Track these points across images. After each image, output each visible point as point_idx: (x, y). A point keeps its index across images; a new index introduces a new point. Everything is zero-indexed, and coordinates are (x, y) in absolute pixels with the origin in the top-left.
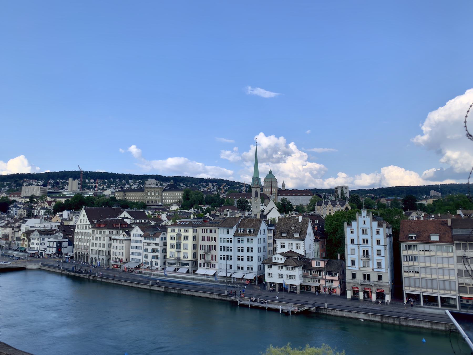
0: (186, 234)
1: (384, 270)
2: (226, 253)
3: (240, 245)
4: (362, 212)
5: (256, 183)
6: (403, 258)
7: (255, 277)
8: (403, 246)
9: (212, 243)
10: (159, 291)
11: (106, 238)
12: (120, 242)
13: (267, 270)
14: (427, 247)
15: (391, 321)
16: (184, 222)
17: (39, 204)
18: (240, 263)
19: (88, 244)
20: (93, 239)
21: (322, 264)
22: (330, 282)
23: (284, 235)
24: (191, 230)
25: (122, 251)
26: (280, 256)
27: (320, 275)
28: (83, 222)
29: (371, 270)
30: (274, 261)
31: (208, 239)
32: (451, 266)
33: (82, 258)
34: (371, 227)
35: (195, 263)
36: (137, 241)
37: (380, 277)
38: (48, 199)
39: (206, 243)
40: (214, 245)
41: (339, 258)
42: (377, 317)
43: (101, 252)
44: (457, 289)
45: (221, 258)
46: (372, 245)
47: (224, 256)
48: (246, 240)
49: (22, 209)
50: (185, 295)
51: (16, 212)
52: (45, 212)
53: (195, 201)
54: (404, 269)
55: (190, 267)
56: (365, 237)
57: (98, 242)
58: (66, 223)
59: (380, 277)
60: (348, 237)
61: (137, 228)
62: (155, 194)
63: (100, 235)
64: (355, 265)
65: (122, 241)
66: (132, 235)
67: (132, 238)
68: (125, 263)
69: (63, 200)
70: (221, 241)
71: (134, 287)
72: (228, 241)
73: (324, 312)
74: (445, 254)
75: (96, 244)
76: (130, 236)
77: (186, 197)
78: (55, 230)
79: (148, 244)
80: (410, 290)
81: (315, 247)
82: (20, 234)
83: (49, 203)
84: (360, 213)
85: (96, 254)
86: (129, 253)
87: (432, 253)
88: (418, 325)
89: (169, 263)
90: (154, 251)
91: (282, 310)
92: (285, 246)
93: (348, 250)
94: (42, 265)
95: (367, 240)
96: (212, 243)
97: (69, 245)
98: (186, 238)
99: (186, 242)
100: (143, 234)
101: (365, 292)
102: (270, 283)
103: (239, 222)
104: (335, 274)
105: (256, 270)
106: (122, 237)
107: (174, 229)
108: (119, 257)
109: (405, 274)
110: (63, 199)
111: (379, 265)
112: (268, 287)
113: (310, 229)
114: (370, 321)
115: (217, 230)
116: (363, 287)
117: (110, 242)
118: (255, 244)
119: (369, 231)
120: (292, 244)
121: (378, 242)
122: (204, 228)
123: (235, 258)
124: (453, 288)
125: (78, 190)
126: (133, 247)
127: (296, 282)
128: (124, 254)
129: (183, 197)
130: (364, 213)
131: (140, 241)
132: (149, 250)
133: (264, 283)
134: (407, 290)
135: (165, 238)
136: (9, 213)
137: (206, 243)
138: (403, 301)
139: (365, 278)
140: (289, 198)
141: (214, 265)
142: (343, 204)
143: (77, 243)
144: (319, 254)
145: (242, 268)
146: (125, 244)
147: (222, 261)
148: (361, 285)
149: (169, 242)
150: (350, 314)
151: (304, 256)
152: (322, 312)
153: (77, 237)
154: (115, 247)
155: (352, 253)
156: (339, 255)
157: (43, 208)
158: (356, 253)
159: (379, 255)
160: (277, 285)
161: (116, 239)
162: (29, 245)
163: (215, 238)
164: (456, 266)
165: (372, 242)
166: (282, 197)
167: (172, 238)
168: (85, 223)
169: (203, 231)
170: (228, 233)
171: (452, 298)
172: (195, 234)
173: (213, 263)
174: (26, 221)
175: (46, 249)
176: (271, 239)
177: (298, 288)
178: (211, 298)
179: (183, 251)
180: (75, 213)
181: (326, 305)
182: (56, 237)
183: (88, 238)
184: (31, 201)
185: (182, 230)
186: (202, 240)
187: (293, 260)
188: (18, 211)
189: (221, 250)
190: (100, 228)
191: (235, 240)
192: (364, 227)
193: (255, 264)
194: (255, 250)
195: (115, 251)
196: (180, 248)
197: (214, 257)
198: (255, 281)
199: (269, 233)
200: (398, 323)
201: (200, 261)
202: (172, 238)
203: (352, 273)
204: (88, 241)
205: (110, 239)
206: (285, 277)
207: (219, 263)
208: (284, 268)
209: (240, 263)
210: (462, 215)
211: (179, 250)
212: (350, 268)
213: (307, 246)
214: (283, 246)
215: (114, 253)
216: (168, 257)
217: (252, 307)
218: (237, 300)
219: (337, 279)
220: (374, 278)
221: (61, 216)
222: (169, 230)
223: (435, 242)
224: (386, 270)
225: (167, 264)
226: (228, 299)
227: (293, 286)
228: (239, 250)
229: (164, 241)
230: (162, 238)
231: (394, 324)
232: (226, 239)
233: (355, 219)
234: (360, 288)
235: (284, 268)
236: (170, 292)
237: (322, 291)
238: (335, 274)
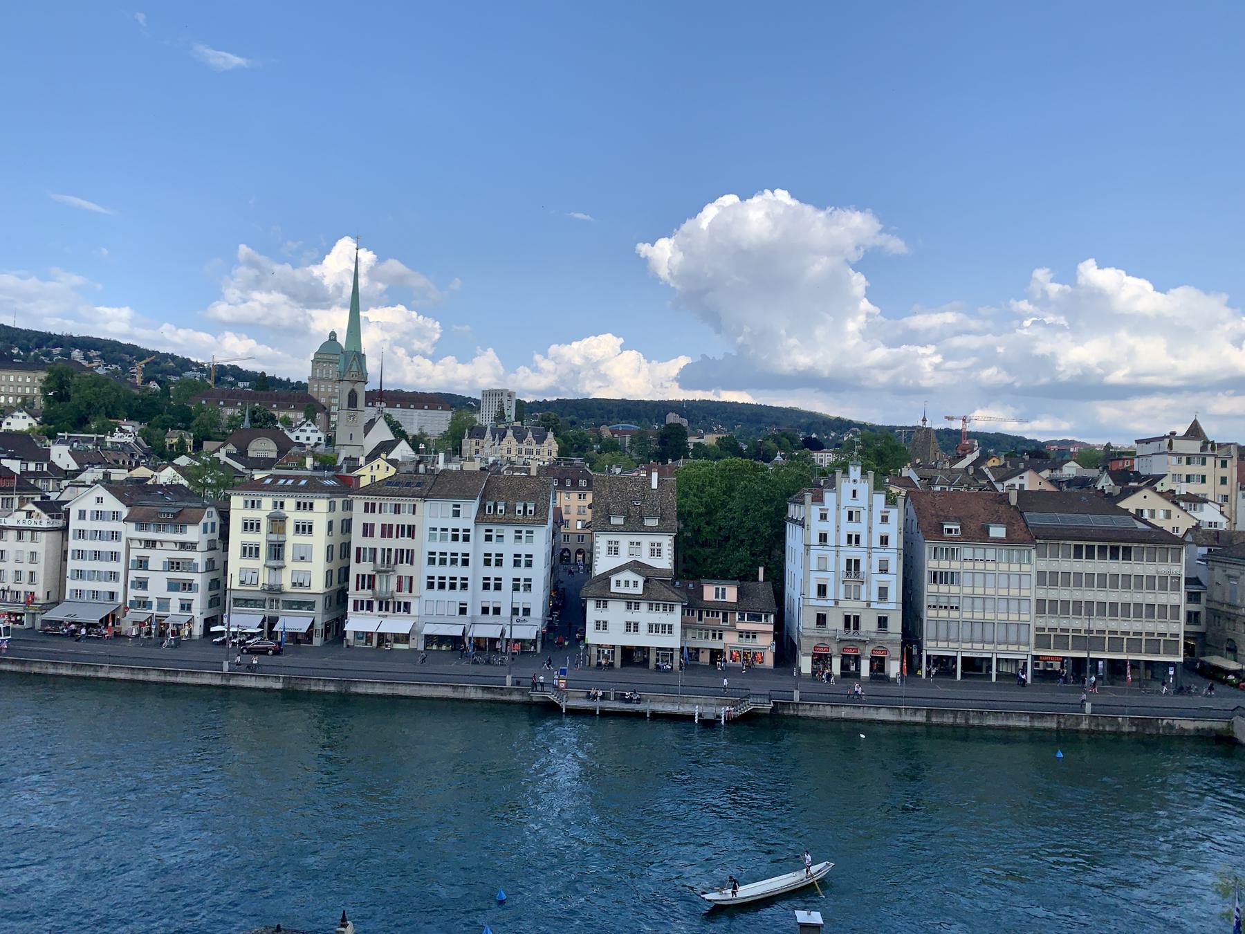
0: (304, 516)
1: (893, 606)
2: (448, 571)
3: (493, 548)
4: (851, 468)
5: (354, 368)
6: (927, 577)
8: (928, 549)
9: (404, 543)
10: (264, 690)
12: (20, 537)
13: (593, 613)
14: (979, 553)
15: (948, 719)
18: (491, 598)
24: (321, 504)
30: (613, 589)
31: (387, 531)
32: (1025, 593)
34: (870, 506)
37: (882, 622)
39: (378, 542)
40: (406, 548)
41: (761, 577)
44: (1033, 640)
45: (431, 586)
48: (513, 534)
50: (367, 695)
53: (89, 405)
54: (928, 600)
56: (853, 528)
59: (882, 622)
65: (27, 535)
66: (74, 515)
70: (432, 538)
72: (455, 538)
74: (1015, 567)
79: (150, 544)
80: (937, 648)
84: (846, 472)
87: (991, 566)
88: (1004, 723)
90: (174, 565)
91: (700, 715)
95: (857, 538)
96: (404, 543)
98: (304, 528)
99: (303, 539)
100: (125, 511)
102: (599, 646)
105: (538, 612)
107: (256, 499)
109: (929, 614)
111: (883, 593)
114: (901, 723)
116: (843, 645)
119: (864, 515)
120: (638, 544)
121: (884, 540)
123: (475, 584)
124: (1023, 638)
126: (80, 554)
127: (673, 641)
128: (40, 578)
130: (855, 472)
131: (115, 536)
134: (931, 647)
139: (847, 625)
141: (407, 605)
145: (497, 611)
147: (436, 593)
150: (856, 711)
156: (761, 570)
158: (831, 567)
159: (883, 570)
160: (618, 653)
164: (1033, 592)
165: (870, 540)
170: (457, 514)
171: (1007, 660)
173: (402, 600)
179: (291, 564)
181: (796, 695)
185: (290, 503)
186: (365, 534)
191: (478, 534)
193: (536, 600)
201: (353, 594)
203: (880, 618)
206: (643, 628)
208: (644, 606)
209: (491, 598)
210: (915, 478)
211: (280, 563)
212: (813, 602)
214: (613, 550)
216: (234, 582)
219: (771, 628)
220: (869, 625)
223: (998, 541)
226: (516, 697)
227: (665, 653)
228: (487, 563)
230: (205, 525)
231: (954, 727)
232: (450, 533)
234: (834, 649)
235: (644, 606)
236: (309, 692)
238: (766, 617)
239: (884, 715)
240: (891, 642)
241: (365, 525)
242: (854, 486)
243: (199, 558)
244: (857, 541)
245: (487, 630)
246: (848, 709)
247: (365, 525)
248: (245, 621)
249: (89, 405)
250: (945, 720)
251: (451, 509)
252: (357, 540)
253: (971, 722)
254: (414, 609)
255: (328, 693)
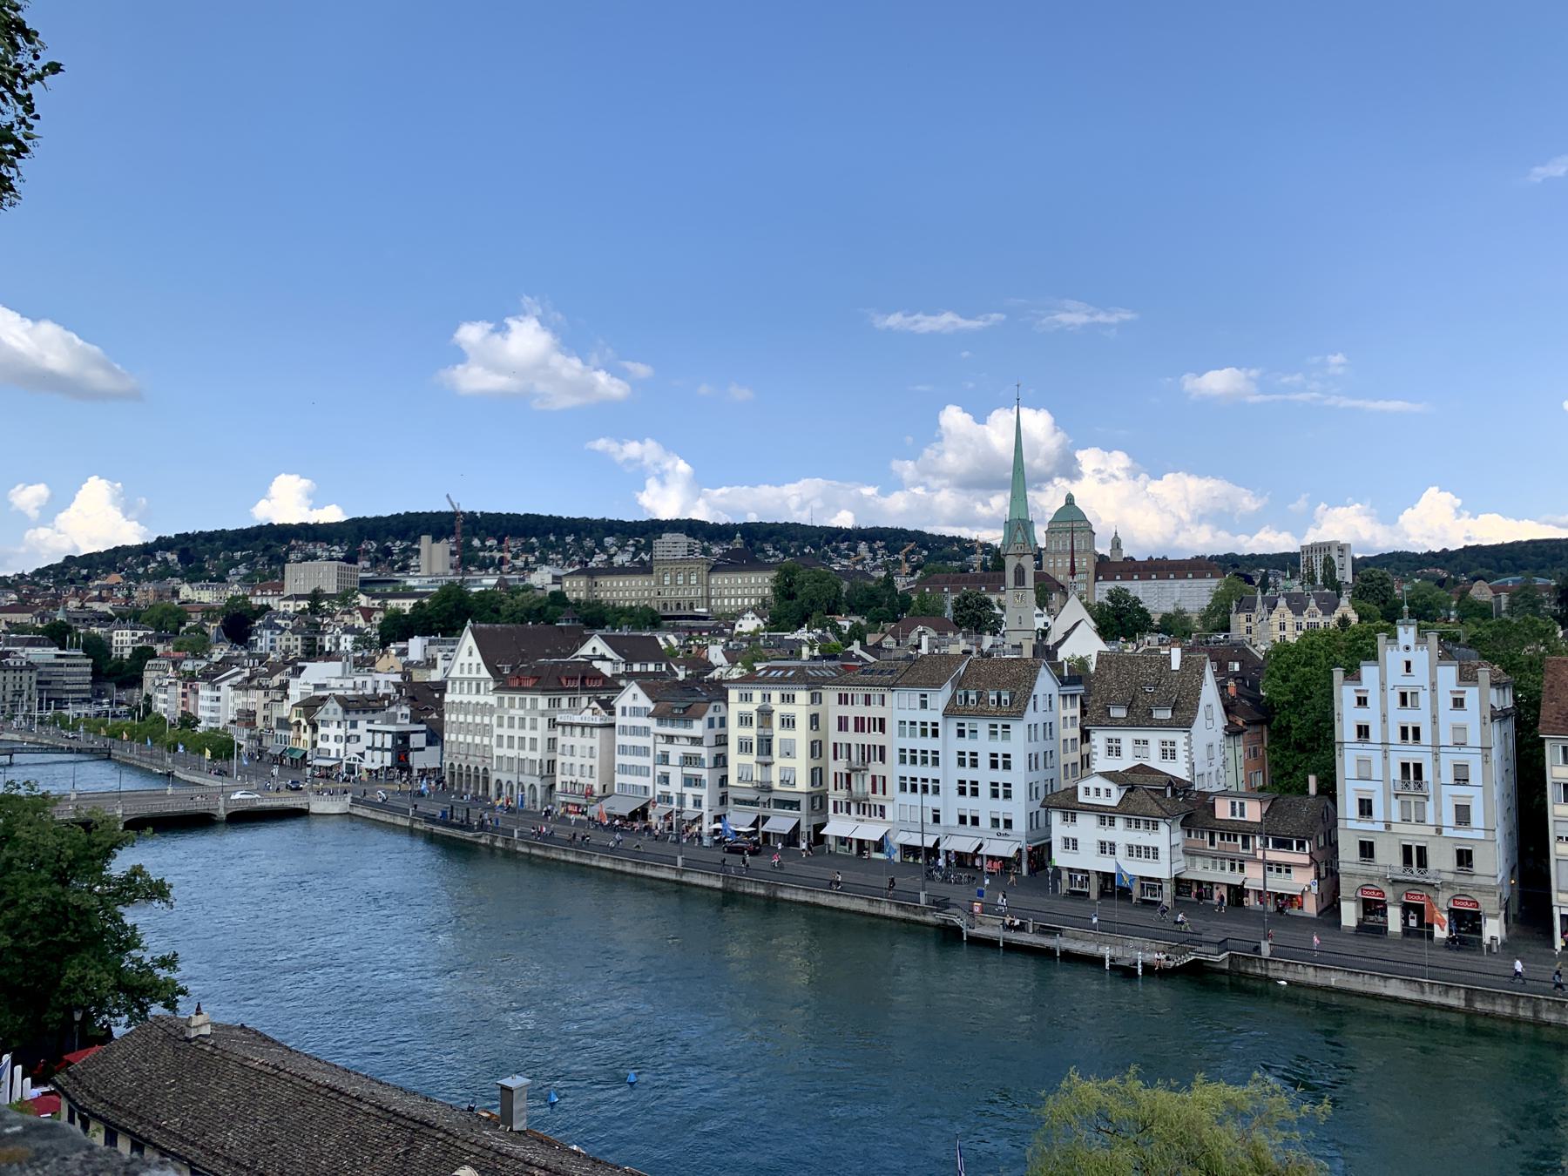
0: (787, 709)
1: (1481, 835)
2: (920, 771)
3: (967, 745)
4: (1401, 630)
5: (1019, 539)
7: (1019, 850)
8: (1552, 753)
9: (874, 738)
11: (540, 719)
13: (1059, 829)
16: (778, 669)
17: (338, 617)
18: (968, 805)
19: (486, 741)
20: (500, 725)
21: (1253, 812)
22: (1279, 871)
23: (1119, 713)
24: (802, 696)
25: (592, 762)
26: (1104, 784)
27: (1246, 846)
28: (470, 671)
29: (1432, 831)
30: (1082, 798)
31: (860, 725)
33: (469, 782)
34: (1433, 684)
35: (818, 801)
36: (635, 731)
37: (1464, 858)
38: (363, 600)
40: (878, 744)
41: (1312, 790)
42: (1451, 993)
43: (527, 764)
45: (903, 788)
46: (1436, 746)
47: (914, 779)
49: (287, 634)
50: (790, 901)
51: (272, 641)
52: (356, 641)
53: (812, 602)
55: (802, 816)
56: (1410, 718)
57: (516, 733)
58: (418, 676)
59: (1464, 858)
60: (1347, 717)
61: (634, 688)
62: (687, 581)
63: (521, 712)
64: (1370, 813)
65: (587, 730)
66: (618, 711)
67: (619, 720)
68: (601, 798)
69: (407, 605)
70: (902, 733)
71: (630, 874)
72: (924, 733)
73: (1259, 971)
75: (511, 738)
76: (612, 714)
77: (785, 591)
78: (387, 696)
79: (670, 739)
81: (1230, 753)
82: (286, 710)
83: (367, 613)
85: (510, 770)
86: (609, 769)
89: (737, 801)
90: (688, 760)
92: (1122, 749)
93: (1348, 762)
94: (354, 800)
95: (1416, 731)
96: (874, 738)
97: (429, 743)
98: (788, 722)
99: (787, 734)
100: (652, 707)
101: (1407, 908)
102: (1070, 870)
103: (962, 669)
104: (1301, 845)
105: (1020, 826)
106: (587, 717)
108: (581, 780)
110: (407, 602)
111: (1463, 815)
112: (1064, 887)
113: (1209, 693)
114: (1427, 1005)
115: (888, 696)
117: (552, 735)
118: (1017, 743)
119: (1424, 698)
120: (1145, 742)
122: (844, 690)
125: (451, 572)
126: (624, 750)
127: (1160, 869)
128: (596, 770)
129: (774, 589)
130: (1407, 633)
132: (674, 759)
133: (1050, 870)
135: (723, 722)
136: (254, 644)
137: (852, 737)
138: (1552, 945)
140: (1136, 588)
141: (882, 808)
142: (1329, 609)
143: (453, 737)
144: (1242, 776)
145: (975, 821)
146: (596, 739)
148: (1395, 881)
149: (735, 732)
150: (1352, 978)
151: (1191, 785)
152: (1250, 970)
153: (454, 718)
154: (568, 749)
155: (1361, 772)
156: (1312, 779)
157: (349, 630)
158: (1377, 773)
160: (1094, 879)
161: (572, 725)
162: (314, 744)
163: (882, 721)
165: (1435, 734)
166: (1110, 585)
167: (745, 720)
168: (474, 675)
169: (843, 700)
170: (924, 705)
172: (815, 709)
174: (303, 669)
175: (362, 755)
176: (1073, 725)
177: (1168, 889)
178: (873, 915)
179: (779, 762)
180: (444, 643)
182: (392, 719)
183: (486, 720)
184: (314, 609)
185: (776, 695)
186: (840, 729)
187: (1147, 795)
188: (278, 638)
189: (903, 760)
190: (521, 689)
192: (1408, 683)
193: (1018, 809)
194: (1019, 762)
195: (568, 759)
196: (769, 752)
197: (879, 784)
198: (1019, 864)
199: (1065, 707)
200: (1529, 1014)
201: (836, 795)
202: (745, 720)
204: (486, 730)
205: (553, 724)
206: (1121, 851)
207: (897, 802)
209: (968, 805)
211: (768, 759)
212: (1351, 825)
213: (1203, 750)
214: (1114, 750)
215: (567, 767)
216: (732, 780)
217: (1010, 947)
218: (958, 921)
219: (1306, 860)
220: (1442, 861)
221: (404, 652)
222: (733, 695)
225: (730, 802)
226: (929, 918)
228: (962, 763)
229: (717, 730)
230: (711, 720)
231: (1514, 1020)
232: (918, 726)
233: (1373, 657)
234: (1389, 895)
236: (744, 894)
237: (1251, 901)
239: (1394, 988)
240: (1480, 889)
241: (840, 718)
243: (704, 752)
245: (963, 843)
246: (1345, 977)
247: (840, 718)
248: (740, 821)
249: (812, 602)
250: (1498, 1008)
251: (918, 699)
252: (834, 736)
253: (1544, 1016)
254: (887, 811)
255: (759, 896)
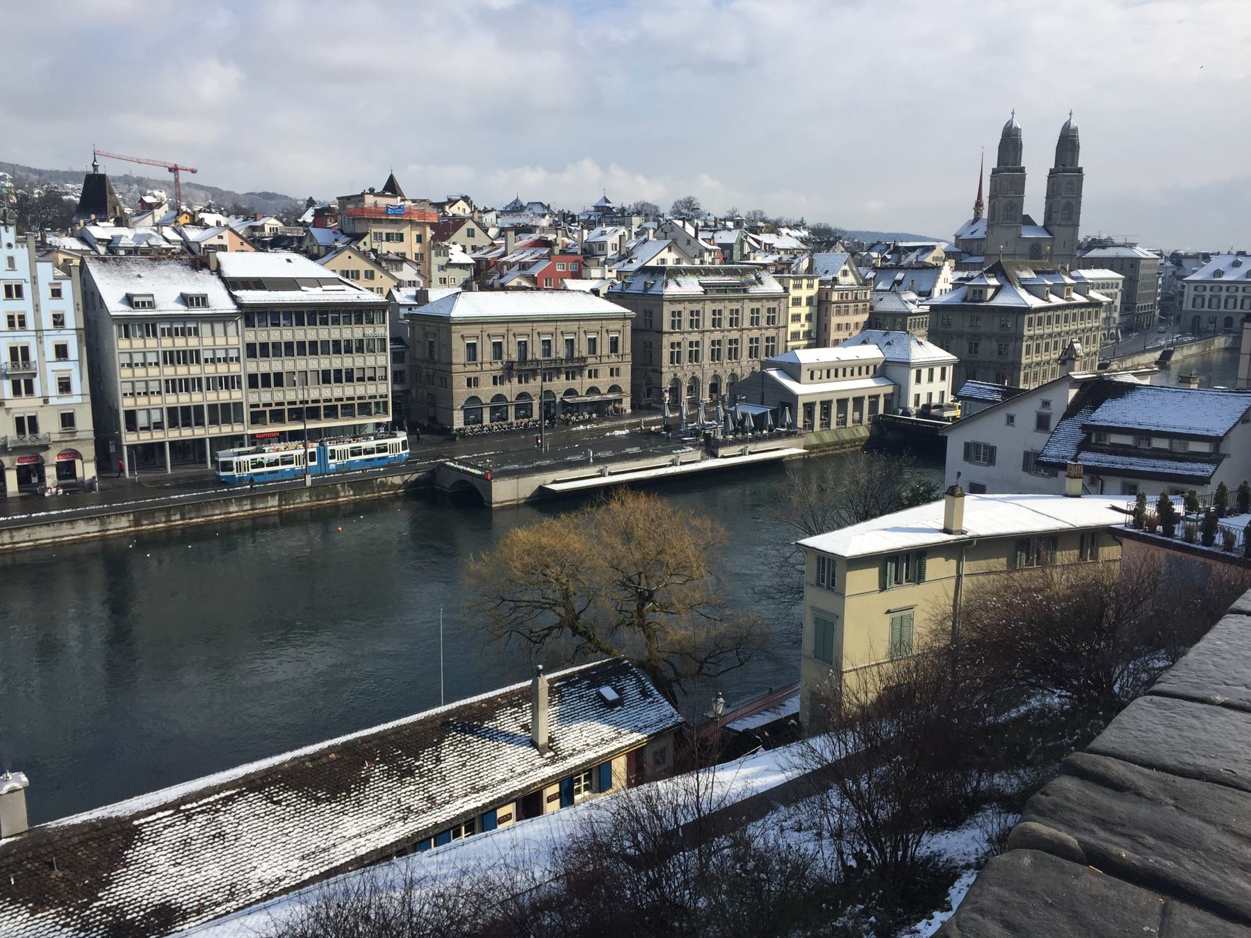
1: (78, 399)
29: (41, 402)
34: (34, 279)
37: (68, 420)
46: (39, 331)
56: (16, 307)
59: (68, 420)
95: (22, 317)
111: (65, 386)
119: (27, 290)
165: (38, 320)
203: (63, 415)
220: (50, 426)
224: (79, 400)
242: (10, 252)
244: (22, 324)
